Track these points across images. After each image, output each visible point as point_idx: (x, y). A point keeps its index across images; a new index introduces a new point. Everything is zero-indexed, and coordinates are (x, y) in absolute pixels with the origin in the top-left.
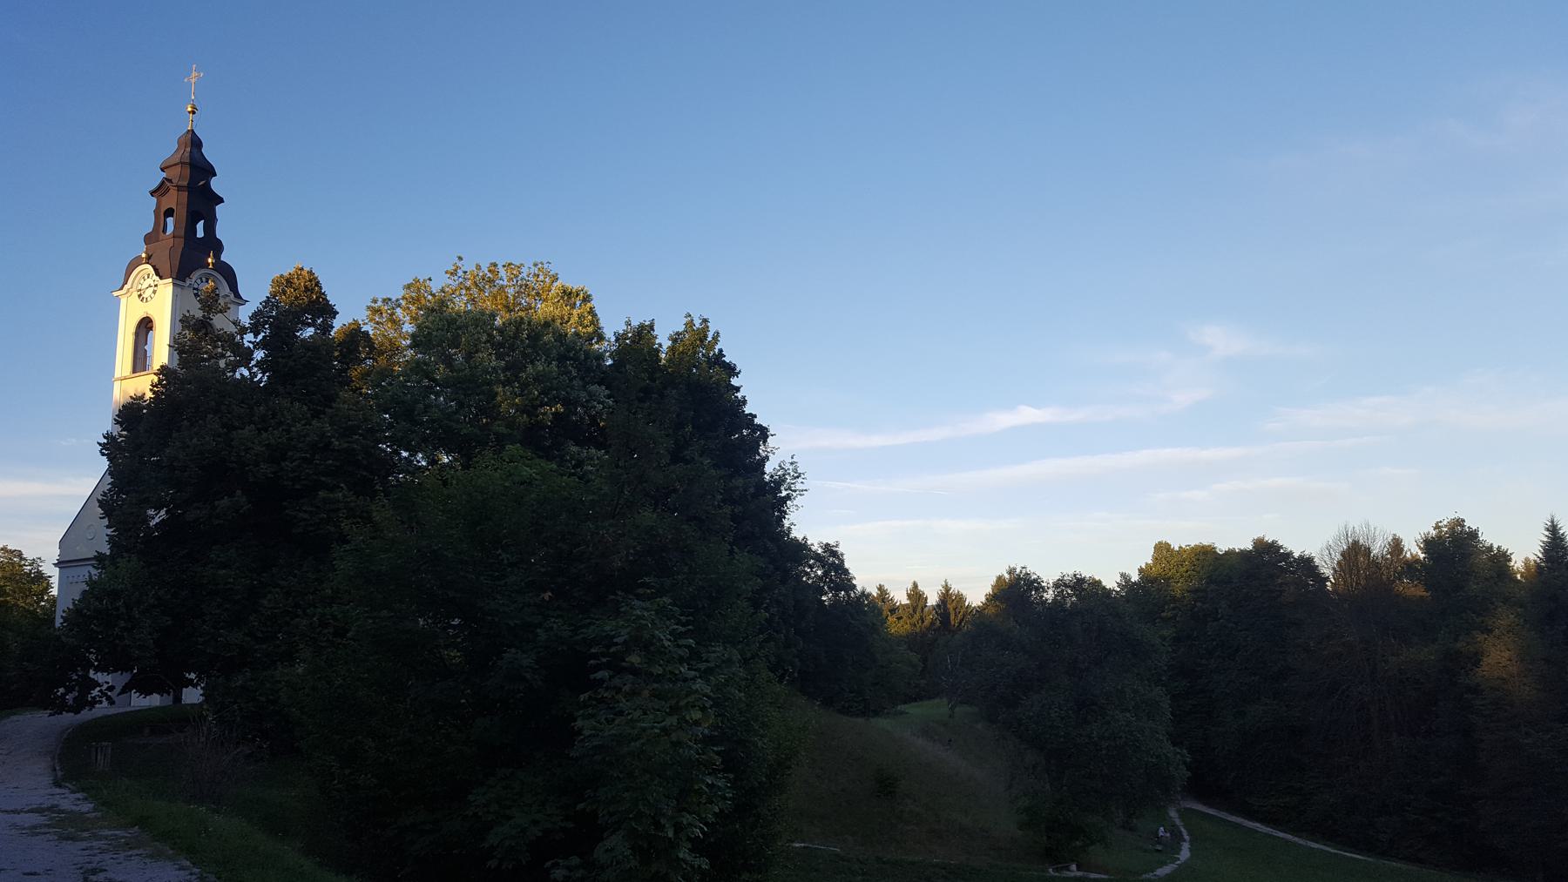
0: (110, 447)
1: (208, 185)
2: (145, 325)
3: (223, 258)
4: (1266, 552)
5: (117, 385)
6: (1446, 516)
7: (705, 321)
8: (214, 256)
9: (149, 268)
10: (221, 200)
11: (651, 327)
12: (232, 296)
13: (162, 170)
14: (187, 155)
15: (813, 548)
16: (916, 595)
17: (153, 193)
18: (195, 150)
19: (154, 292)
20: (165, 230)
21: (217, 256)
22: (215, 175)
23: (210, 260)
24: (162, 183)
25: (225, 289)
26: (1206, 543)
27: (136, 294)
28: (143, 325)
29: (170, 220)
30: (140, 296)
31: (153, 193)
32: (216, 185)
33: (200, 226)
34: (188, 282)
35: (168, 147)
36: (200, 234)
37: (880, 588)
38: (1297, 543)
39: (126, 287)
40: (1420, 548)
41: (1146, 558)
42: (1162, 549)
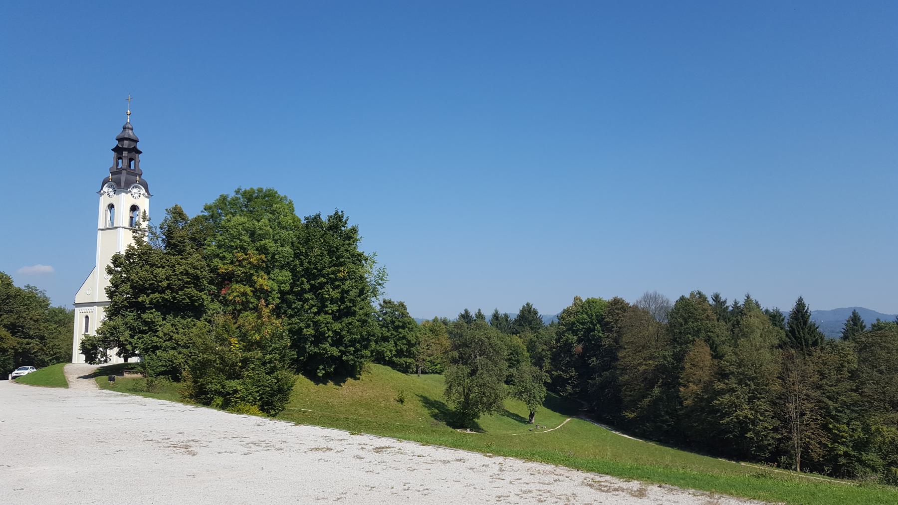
0: (110, 271)
1: (135, 147)
2: (111, 206)
3: (142, 177)
4: (616, 302)
5: (100, 232)
6: (695, 289)
7: (342, 212)
8: (139, 177)
9: (113, 184)
10: (141, 152)
11: (320, 215)
12: (146, 194)
13: (116, 140)
14: (127, 134)
15: (395, 303)
16: (480, 316)
17: (113, 150)
18: (130, 132)
19: (114, 193)
20: (117, 165)
21: (140, 175)
22: (138, 141)
23: (138, 180)
24: (117, 145)
25: (144, 191)
26: (596, 297)
27: (106, 194)
28: (110, 206)
29: (120, 161)
30: (108, 194)
31: (113, 150)
32: (139, 146)
33: (132, 163)
34: (129, 190)
35: (118, 132)
36: (132, 167)
37: (466, 311)
38: (631, 299)
39: (102, 191)
40: (714, 300)
41: (569, 303)
42: (576, 298)
